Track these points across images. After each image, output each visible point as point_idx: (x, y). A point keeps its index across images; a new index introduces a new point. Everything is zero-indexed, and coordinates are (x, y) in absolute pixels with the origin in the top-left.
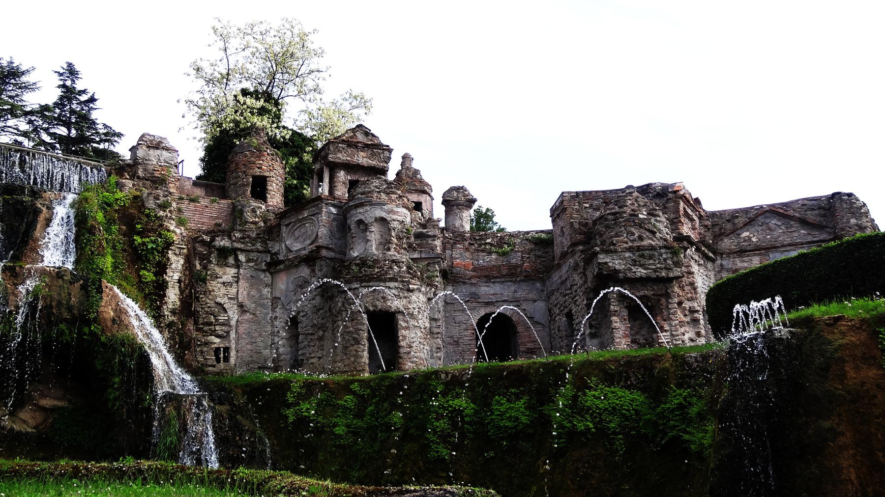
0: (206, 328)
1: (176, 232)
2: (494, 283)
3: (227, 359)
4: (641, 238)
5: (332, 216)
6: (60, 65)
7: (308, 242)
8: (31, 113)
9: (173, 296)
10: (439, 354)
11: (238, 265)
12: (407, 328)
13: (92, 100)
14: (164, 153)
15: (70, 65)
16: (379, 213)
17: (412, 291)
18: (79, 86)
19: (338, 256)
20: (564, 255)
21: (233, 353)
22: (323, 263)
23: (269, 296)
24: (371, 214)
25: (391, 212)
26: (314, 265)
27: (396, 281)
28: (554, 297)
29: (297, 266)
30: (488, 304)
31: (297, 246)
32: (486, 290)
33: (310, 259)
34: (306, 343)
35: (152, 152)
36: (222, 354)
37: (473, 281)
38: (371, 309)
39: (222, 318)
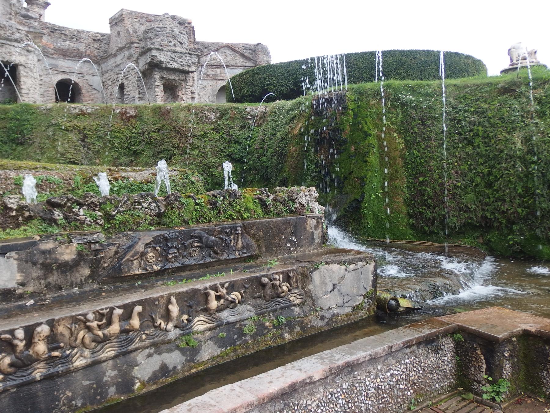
2: (68, 60)
12: (26, 77)
20: (121, 49)
28: (107, 75)
32: (64, 64)
37: (55, 56)
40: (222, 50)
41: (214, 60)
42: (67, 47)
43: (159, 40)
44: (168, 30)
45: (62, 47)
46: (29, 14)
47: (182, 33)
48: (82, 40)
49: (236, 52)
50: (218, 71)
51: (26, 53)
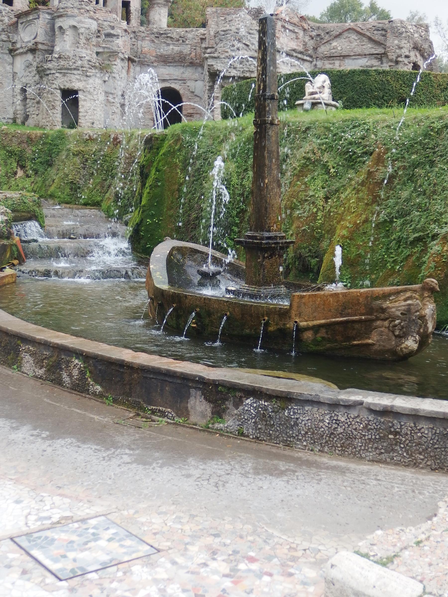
2: (169, 66)
5: (47, 21)
7: (33, 37)
10: (113, 117)
12: (85, 100)
16: (72, 22)
17: (89, 76)
19: (50, 48)
22: (40, 53)
23: (11, 71)
26: (35, 54)
27: (78, 70)
29: (26, 53)
31: (26, 39)
33: (33, 51)
34: (30, 104)
37: (155, 64)
38: (62, 87)
40: (346, 34)
41: (334, 49)
42: (169, 52)
43: (222, 45)
44: (232, 33)
45: (165, 53)
46: (112, 32)
47: (250, 33)
48: (187, 42)
49: (364, 35)
50: (337, 63)
51: (85, 78)
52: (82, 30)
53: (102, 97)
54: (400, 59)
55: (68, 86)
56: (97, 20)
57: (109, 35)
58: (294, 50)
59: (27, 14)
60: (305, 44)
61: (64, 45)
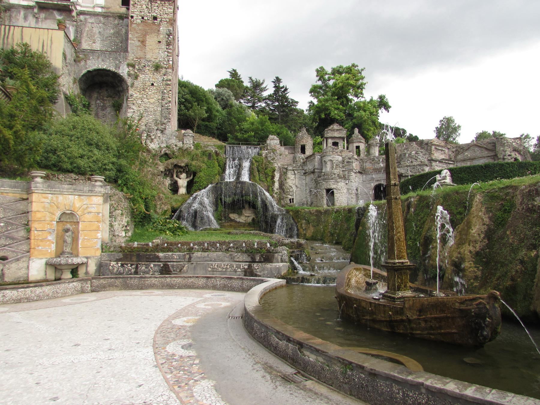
0: (288, 193)
1: (277, 165)
3: (293, 202)
4: (412, 162)
6: (273, 79)
8: (265, 99)
9: (277, 185)
11: (295, 174)
13: (286, 90)
14: (275, 141)
15: (277, 78)
16: (330, 158)
18: (281, 85)
21: (295, 200)
24: (327, 159)
25: (334, 157)
30: (378, 181)
31: (311, 168)
33: (313, 172)
35: (272, 141)
36: (291, 200)
39: (291, 190)
52: (334, 161)
53: (345, 191)
54: (505, 157)
55: (328, 187)
56: (341, 156)
57: (348, 162)
58: (443, 159)
59: (310, 156)
60: (450, 155)
61: (328, 168)
